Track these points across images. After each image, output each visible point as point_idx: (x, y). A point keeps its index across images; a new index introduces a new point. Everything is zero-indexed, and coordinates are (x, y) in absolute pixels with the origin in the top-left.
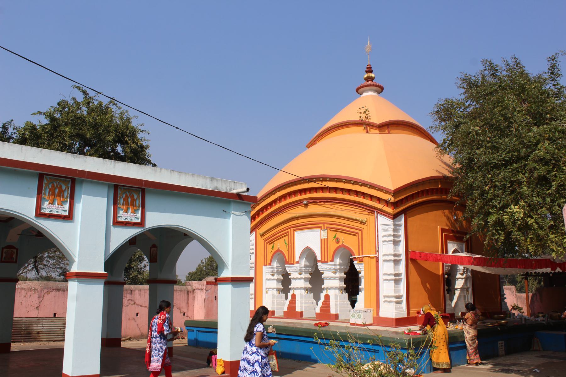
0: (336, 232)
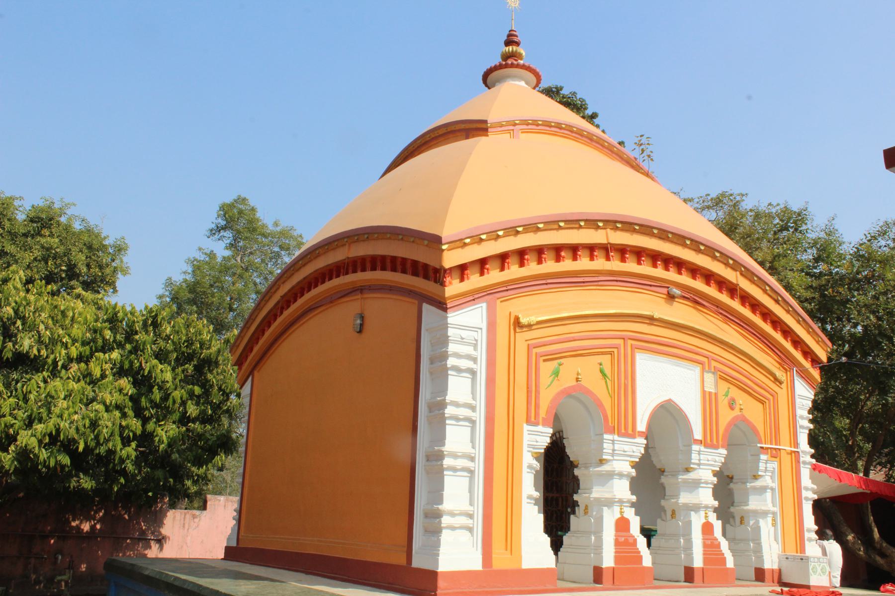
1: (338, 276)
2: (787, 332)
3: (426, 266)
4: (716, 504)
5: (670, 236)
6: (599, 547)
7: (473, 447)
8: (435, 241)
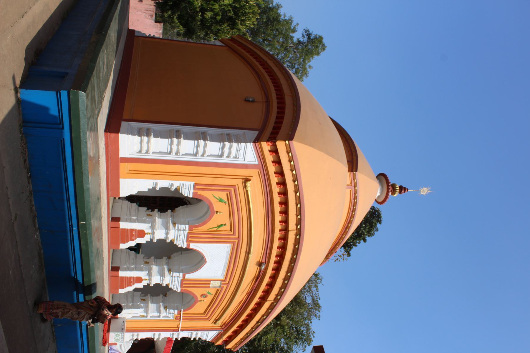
0: (214, 294)
1: (276, 90)
2: (241, 328)
3: (277, 133)
4: (152, 285)
5: (292, 264)
6: (130, 221)
7: (183, 155)
8: (291, 137)
